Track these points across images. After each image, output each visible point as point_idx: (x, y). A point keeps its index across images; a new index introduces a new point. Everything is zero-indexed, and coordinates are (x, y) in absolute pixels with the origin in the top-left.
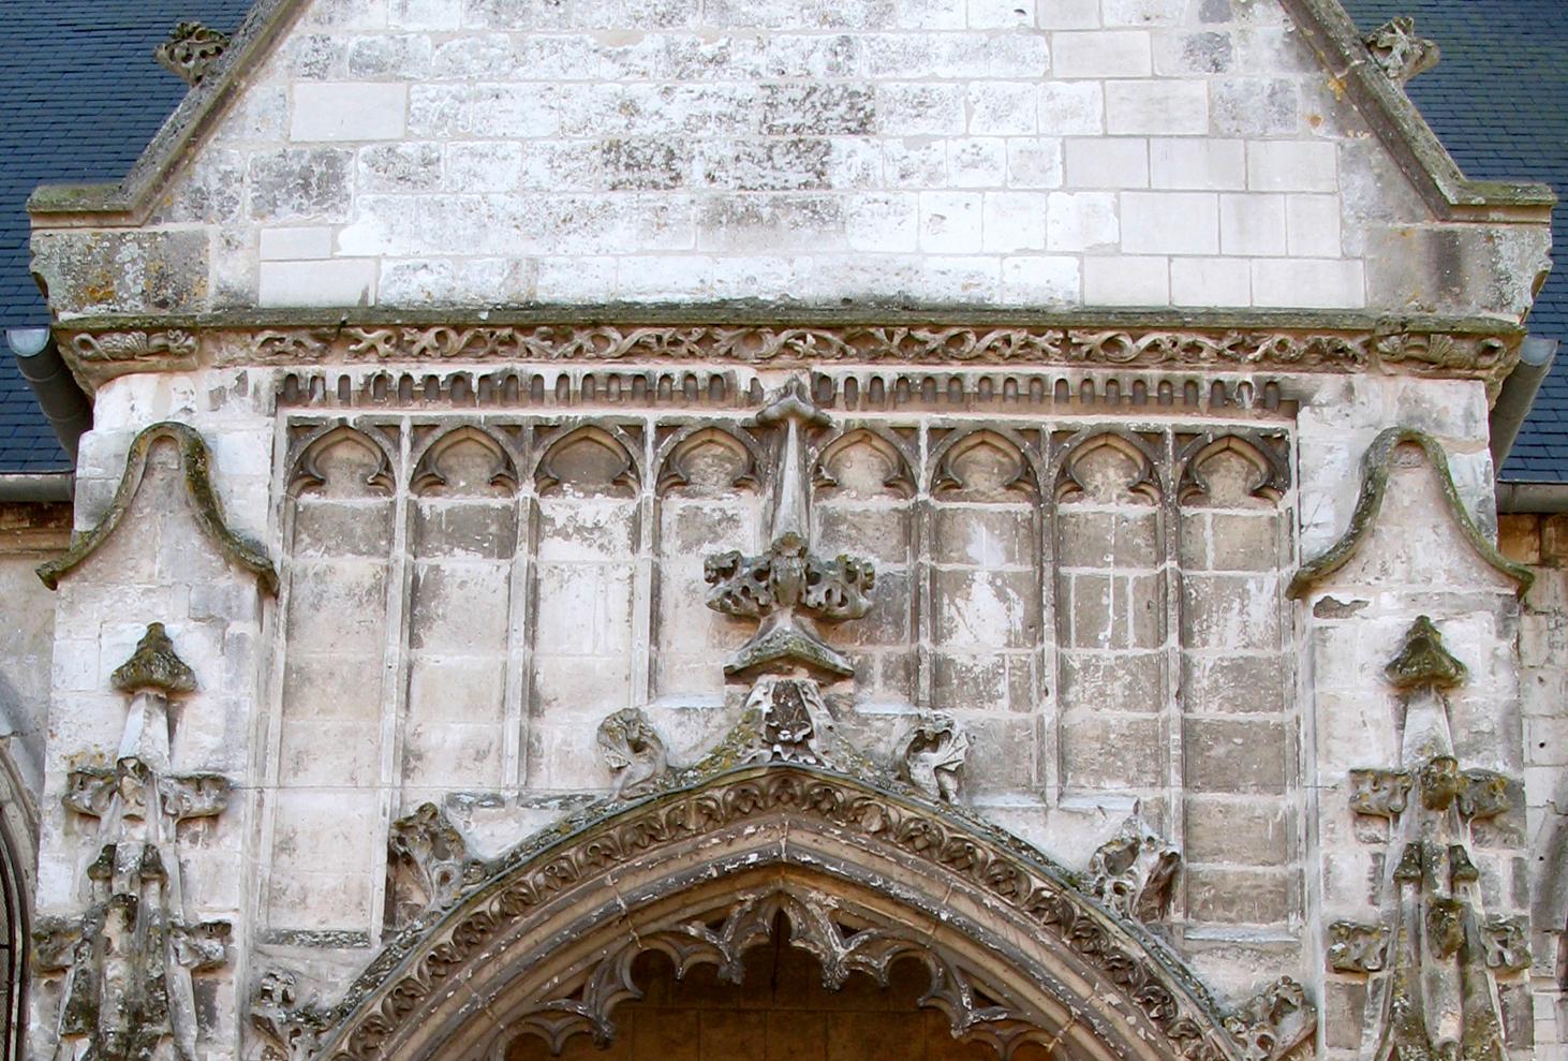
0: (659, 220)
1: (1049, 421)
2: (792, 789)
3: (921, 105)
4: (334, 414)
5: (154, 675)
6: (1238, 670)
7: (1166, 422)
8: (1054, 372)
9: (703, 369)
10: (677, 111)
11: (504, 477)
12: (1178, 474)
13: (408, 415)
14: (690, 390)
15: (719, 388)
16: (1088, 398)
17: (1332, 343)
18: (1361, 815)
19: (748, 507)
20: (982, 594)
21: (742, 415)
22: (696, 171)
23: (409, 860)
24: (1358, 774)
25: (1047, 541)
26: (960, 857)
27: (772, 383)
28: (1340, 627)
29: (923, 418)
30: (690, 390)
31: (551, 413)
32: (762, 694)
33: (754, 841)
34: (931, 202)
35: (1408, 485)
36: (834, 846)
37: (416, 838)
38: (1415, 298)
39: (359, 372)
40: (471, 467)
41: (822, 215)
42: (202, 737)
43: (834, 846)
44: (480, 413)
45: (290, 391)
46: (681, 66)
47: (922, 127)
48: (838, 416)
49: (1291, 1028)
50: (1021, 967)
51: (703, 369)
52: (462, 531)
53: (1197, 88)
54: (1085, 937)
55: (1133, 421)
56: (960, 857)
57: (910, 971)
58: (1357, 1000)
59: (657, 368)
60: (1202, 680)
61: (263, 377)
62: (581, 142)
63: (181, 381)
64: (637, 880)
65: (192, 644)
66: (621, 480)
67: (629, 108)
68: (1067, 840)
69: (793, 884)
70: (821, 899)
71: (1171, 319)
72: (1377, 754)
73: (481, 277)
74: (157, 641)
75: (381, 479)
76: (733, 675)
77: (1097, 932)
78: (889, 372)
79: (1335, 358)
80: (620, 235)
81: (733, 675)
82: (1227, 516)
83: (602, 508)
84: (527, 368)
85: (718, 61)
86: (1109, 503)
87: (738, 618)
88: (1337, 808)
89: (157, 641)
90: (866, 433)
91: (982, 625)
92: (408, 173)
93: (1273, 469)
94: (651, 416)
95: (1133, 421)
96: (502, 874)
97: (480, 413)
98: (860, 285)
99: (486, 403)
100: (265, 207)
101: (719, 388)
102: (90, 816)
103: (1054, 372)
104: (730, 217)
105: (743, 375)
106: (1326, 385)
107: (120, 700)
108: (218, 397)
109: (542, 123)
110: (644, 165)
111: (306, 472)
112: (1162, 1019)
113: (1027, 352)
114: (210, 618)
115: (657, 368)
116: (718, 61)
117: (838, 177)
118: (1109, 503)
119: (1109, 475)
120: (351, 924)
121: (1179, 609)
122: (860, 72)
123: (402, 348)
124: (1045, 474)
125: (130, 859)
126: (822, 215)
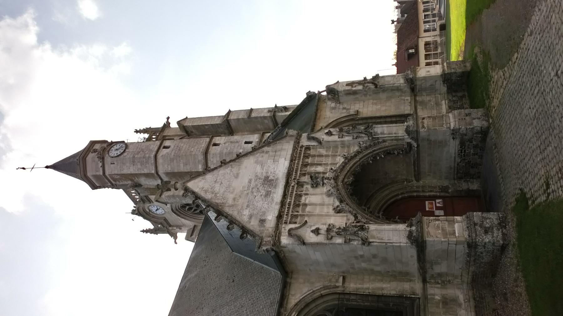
0: (274, 193)
1: (301, 163)
2: (336, 179)
3: (267, 173)
4: (289, 220)
5: (317, 232)
6: (326, 151)
7: (302, 155)
8: (296, 162)
9: (291, 188)
10: (263, 191)
11: (298, 206)
12: (307, 156)
13: (290, 213)
14: (293, 189)
15: (293, 187)
16: (299, 160)
17: (297, 142)
18: (342, 137)
19: (305, 186)
20: (317, 169)
21: (296, 186)
22: (270, 189)
23: (340, 210)
24: (339, 138)
25: (312, 165)
26: (344, 167)
27: (293, 183)
28: (325, 140)
29: (299, 172)
30: (288, 210)
31: (293, 201)
32: (325, 181)
33: (340, 183)
34: (277, 172)
35: (313, 135)
36: (341, 178)
37: (338, 211)
38: (294, 138)
39: (285, 216)
40: (297, 209)
41: (277, 179)
42: (324, 228)
43: (341, 178)
44: (292, 207)
45: (286, 223)
46: (258, 191)
47: (270, 173)
48: (298, 178)
49: (361, 143)
50: (355, 164)
51: (291, 188)
52: (304, 210)
53: (271, 153)
54: (352, 158)
55: (302, 157)
56: (344, 167)
57: (353, 175)
58: (360, 137)
59: (290, 191)
60: (327, 154)
61: (283, 226)
62: (264, 199)
63: (282, 234)
64: (343, 192)
65: (314, 228)
66: (300, 196)
67: (261, 195)
68: (342, 160)
69: (344, 182)
70: (346, 180)
71: (292, 155)
72: (337, 137)
73: (278, 207)
74: (313, 231)
75: (296, 216)
76: (323, 185)
77: (351, 157)
78: (294, 174)
79: (299, 143)
80: (275, 196)
81: (323, 185)
82: (312, 152)
83: (303, 198)
84: (288, 202)
85: (258, 189)
86: (310, 160)
87: (316, 186)
88: (341, 139)
89: (313, 231)
90: (300, 177)
91: (320, 169)
92: (264, 213)
93: (308, 148)
94: (295, 193)
95: (302, 157)
96: (341, 202)
97: (292, 207)
98: (285, 176)
99: (291, 208)
100: (264, 226)
101: (293, 187)
102: (332, 237)
103: (296, 162)
104: (275, 187)
105: (292, 185)
106: (301, 144)
107: (319, 236)
108: (285, 230)
109: (261, 202)
110: (268, 194)
111: (295, 223)
112: (360, 152)
113: (294, 163)
114: (311, 226)
115: (290, 191)
116: (258, 189)
117: (273, 178)
118: (310, 160)
119: (307, 160)
120: (345, 218)
121: (321, 156)
122: (263, 177)
123: (283, 212)
124: (306, 165)
125: (337, 231)
126: (277, 179)
